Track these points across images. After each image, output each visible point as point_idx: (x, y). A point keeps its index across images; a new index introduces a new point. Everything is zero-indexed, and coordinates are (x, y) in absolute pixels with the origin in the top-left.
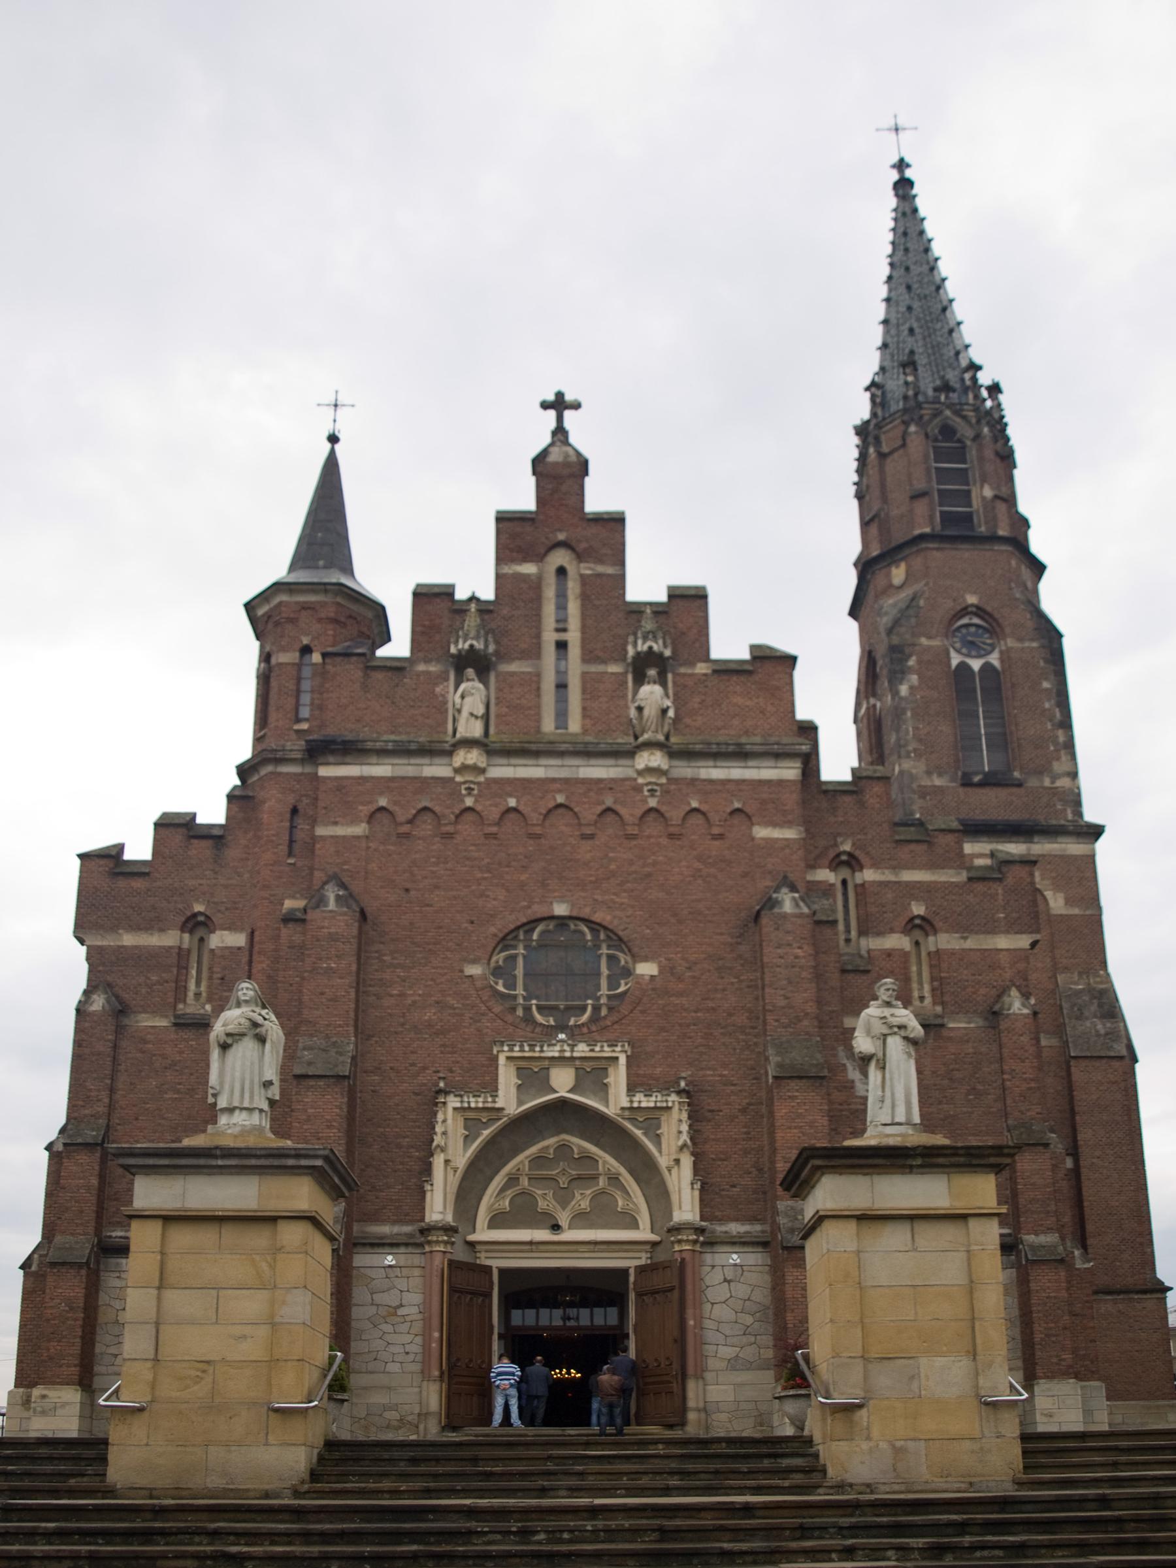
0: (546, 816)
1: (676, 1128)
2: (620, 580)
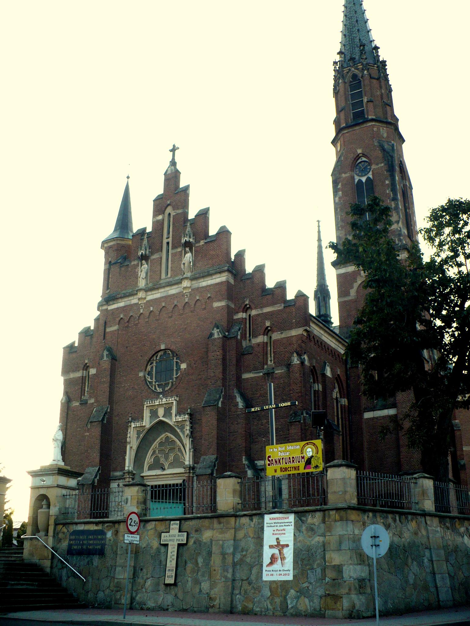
2: (186, 214)
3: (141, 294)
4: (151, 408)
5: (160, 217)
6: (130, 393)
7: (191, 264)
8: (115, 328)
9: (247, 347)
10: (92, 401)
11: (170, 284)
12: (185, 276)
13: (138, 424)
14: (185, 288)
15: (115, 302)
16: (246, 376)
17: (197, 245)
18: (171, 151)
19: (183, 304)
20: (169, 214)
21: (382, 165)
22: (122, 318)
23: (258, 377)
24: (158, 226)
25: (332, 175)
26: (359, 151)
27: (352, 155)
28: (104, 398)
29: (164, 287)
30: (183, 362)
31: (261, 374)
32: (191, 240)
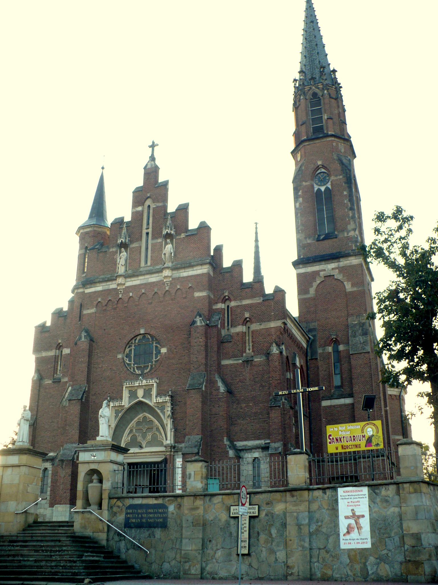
0: (139, 298)
1: (168, 410)
2: (165, 207)
3: (120, 280)
4: (130, 389)
5: (140, 209)
6: (108, 374)
7: (173, 255)
8: (93, 310)
9: (225, 336)
10: (66, 379)
11: (150, 273)
12: (166, 265)
13: (117, 404)
14: (165, 277)
15: (92, 286)
16: (225, 362)
17: (178, 237)
18: (150, 147)
19: (163, 292)
20: (149, 206)
21: (341, 177)
22: (99, 302)
23: (237, 364)
24: (137, 217)
25: (293, 182)
26: (320, 163)
27: (313, 166)
28: (82, 377)
29: (144, 275)
30: (163, 347)
31: (241, 361)
32: (172, 232)
